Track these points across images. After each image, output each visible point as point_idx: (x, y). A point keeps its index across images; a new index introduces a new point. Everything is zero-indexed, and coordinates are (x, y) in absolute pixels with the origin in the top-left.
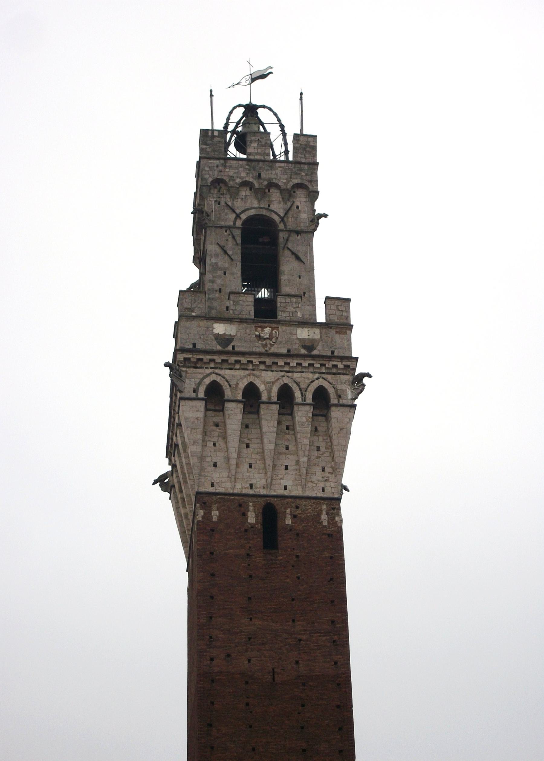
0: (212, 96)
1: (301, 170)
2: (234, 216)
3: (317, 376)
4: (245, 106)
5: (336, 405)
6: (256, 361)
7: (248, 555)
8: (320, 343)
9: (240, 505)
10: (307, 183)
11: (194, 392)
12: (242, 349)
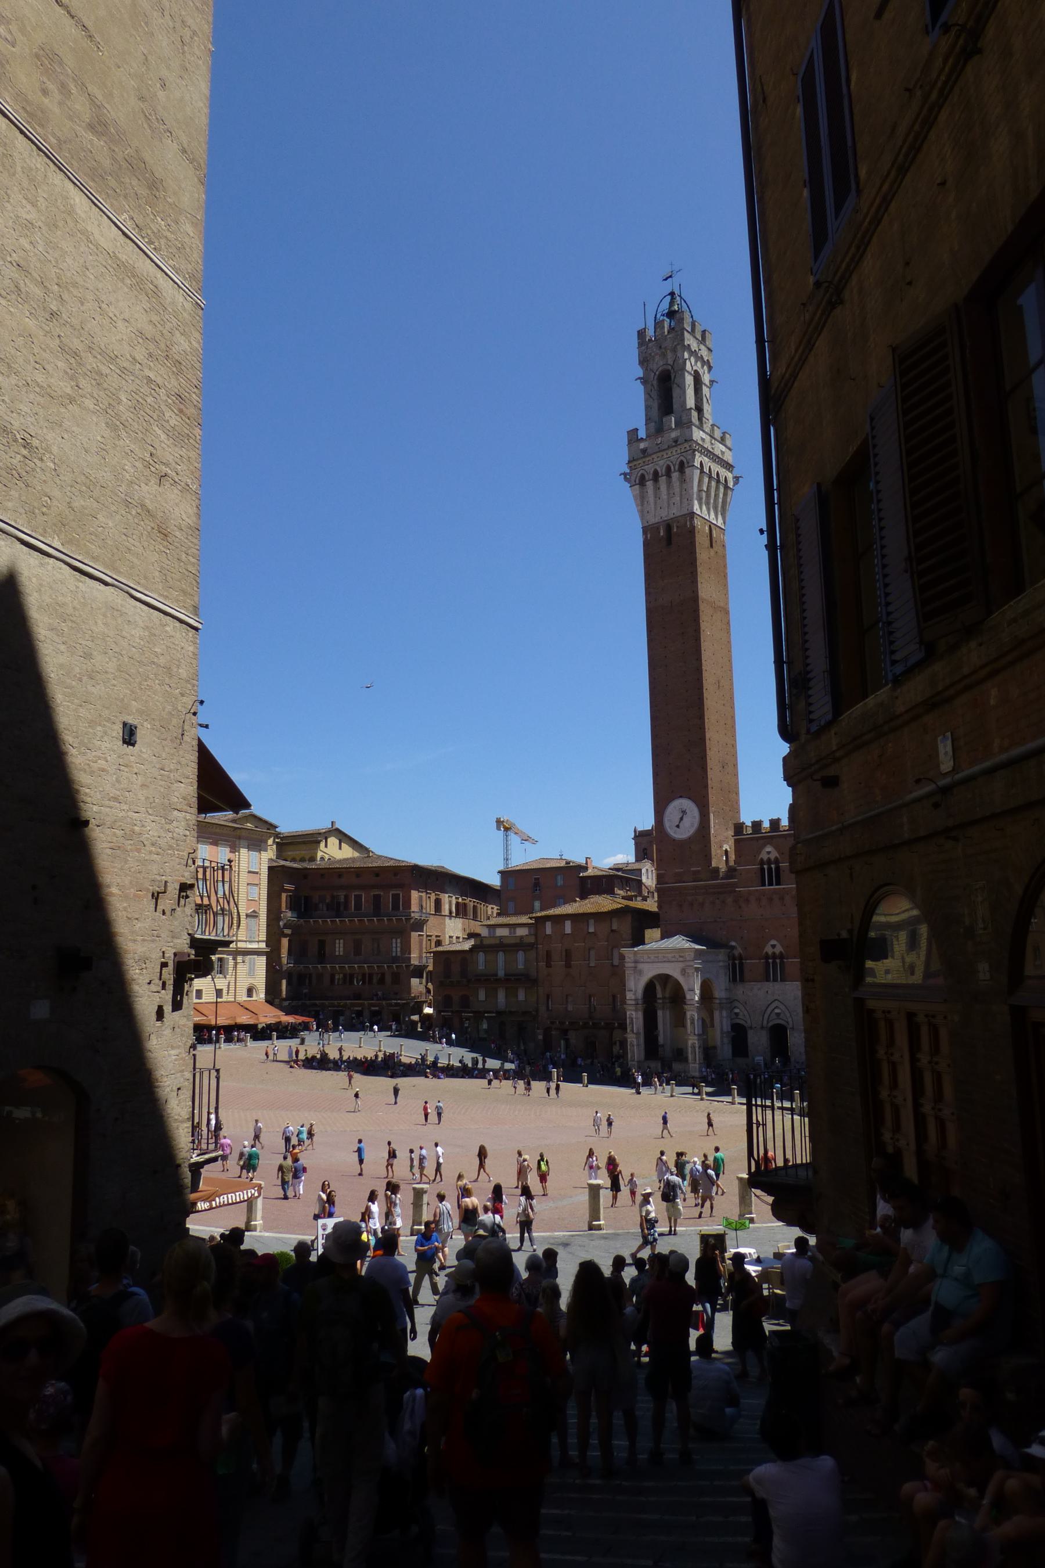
4: (669, 294)
11: (635, 481)
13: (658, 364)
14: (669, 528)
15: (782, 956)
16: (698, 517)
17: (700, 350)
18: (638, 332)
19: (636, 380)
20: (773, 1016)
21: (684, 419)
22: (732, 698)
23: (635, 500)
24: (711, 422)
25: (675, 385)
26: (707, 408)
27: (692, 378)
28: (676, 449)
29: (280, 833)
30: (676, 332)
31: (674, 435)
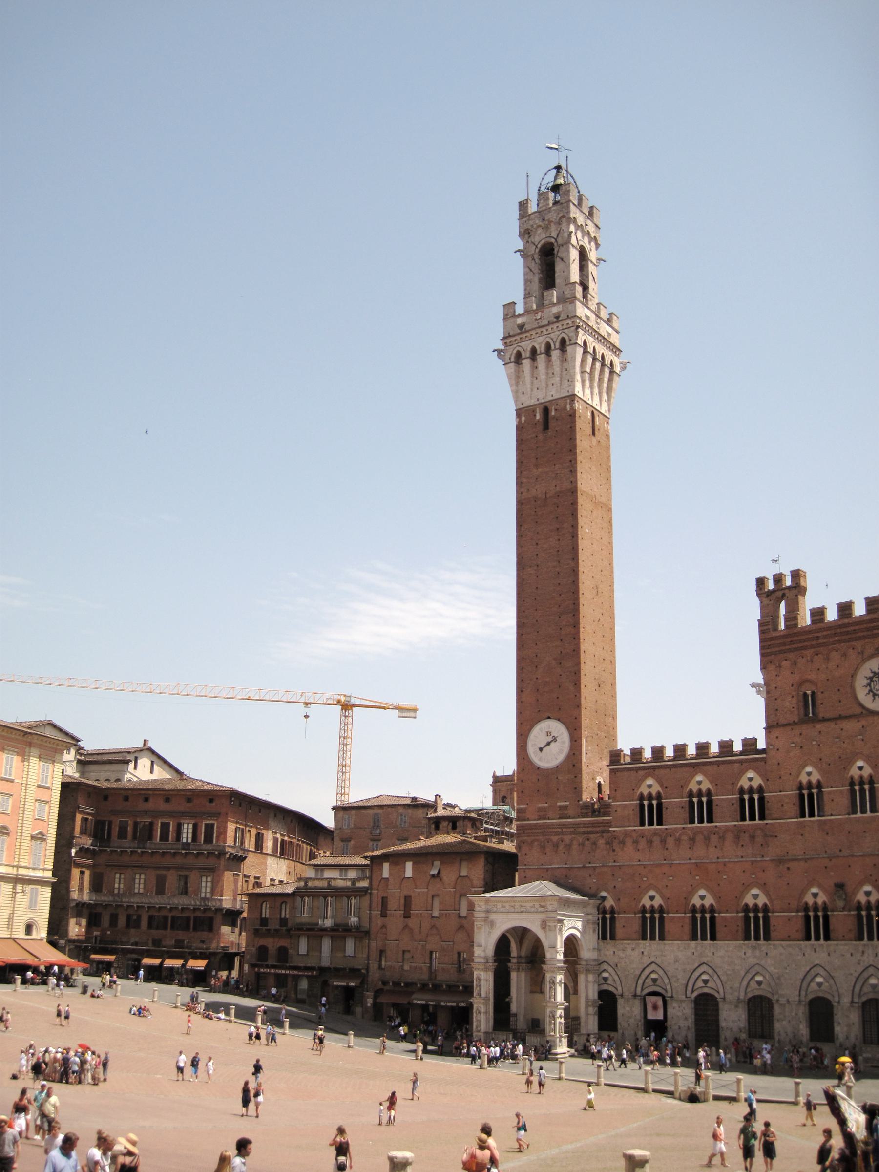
0: (528, 176)
1: (563, 208)
2: (535, 247)
3: (561, 331)
4: (555, 168)
5: (569, 345)
6: (533, 332)
7: (537, 436)
8: (563, 313)
9: (533, 411)
10: (565, 215)
11: (510, 359)
12: (529, 328)
13: (540, 238)
14: (546, 411)
15: (661, 910)
16: (580, 401)
17: (586, 225)
18: (520, 203)
19: (515, 252)
20: (649, 982)
21: (568, 293)
22: (612, 607)
23: (509, 378)
24: (597, 301)
25: (558, 259)
26: (591, 285)
27: (578, 252)
28: (557, 325)
29: (82, 748)
30: (562, 204)
31: (555, 310)
